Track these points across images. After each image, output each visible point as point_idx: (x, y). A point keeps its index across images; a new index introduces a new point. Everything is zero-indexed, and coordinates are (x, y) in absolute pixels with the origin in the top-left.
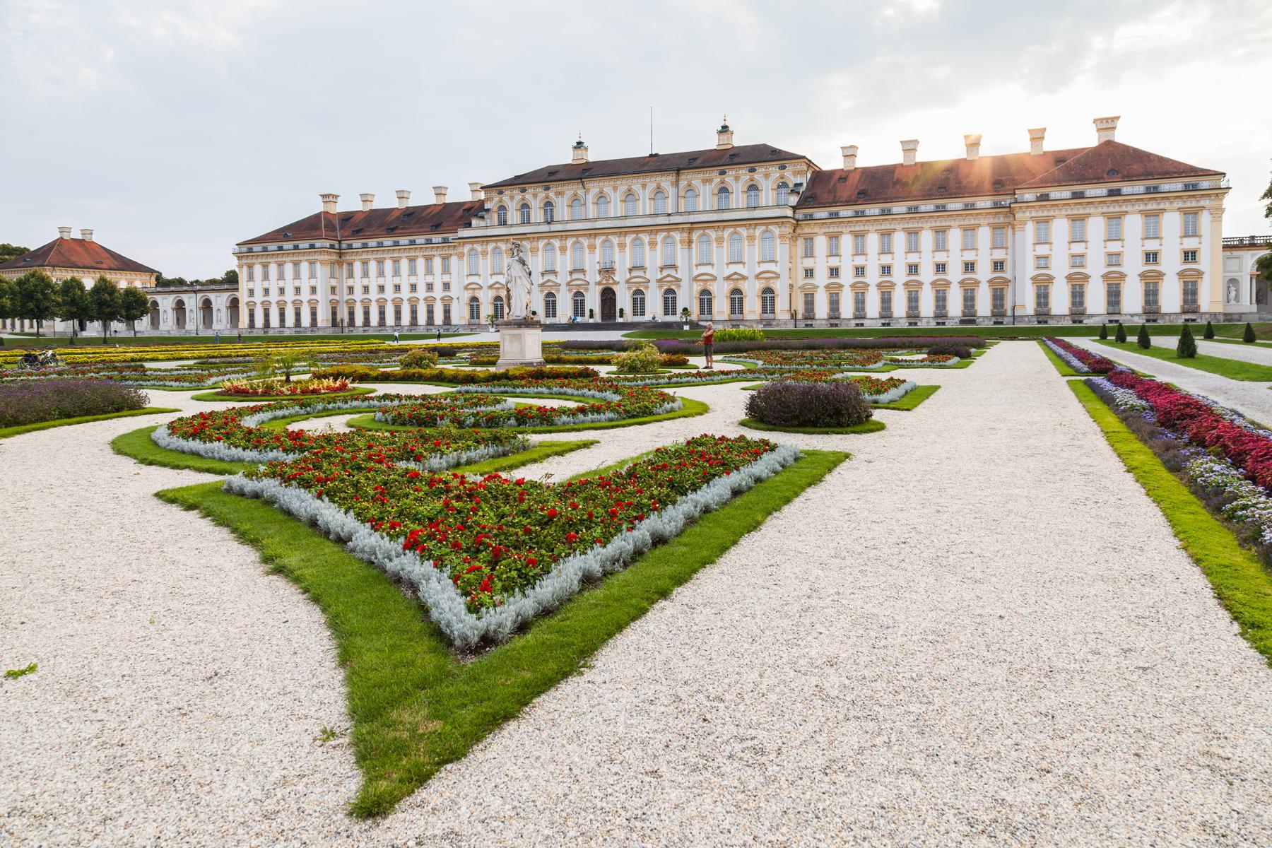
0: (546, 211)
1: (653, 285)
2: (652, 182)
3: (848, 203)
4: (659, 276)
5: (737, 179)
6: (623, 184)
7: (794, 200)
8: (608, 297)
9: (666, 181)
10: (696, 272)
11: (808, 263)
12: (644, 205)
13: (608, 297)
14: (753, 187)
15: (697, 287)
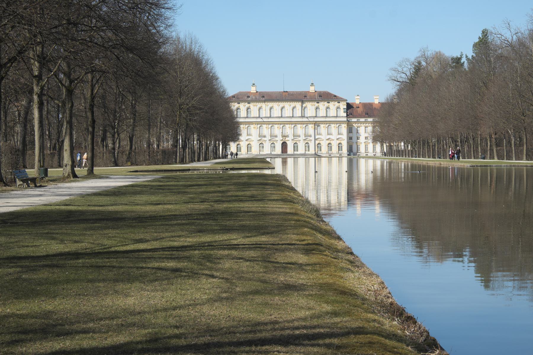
0: (247, 112)
1: (302, 141)
2: (293, 104)
3: (361, 117)
4: (304, 138)
5: (323, 105)
6: (282, 104)
7: (345, 115)
8: (284, 146)
9: (298, 105)
10: (316, 138)
11: (351, 135)
12: (288, 112)
13: (284, 146)
14: (328, 108)
15: (317, 142)
